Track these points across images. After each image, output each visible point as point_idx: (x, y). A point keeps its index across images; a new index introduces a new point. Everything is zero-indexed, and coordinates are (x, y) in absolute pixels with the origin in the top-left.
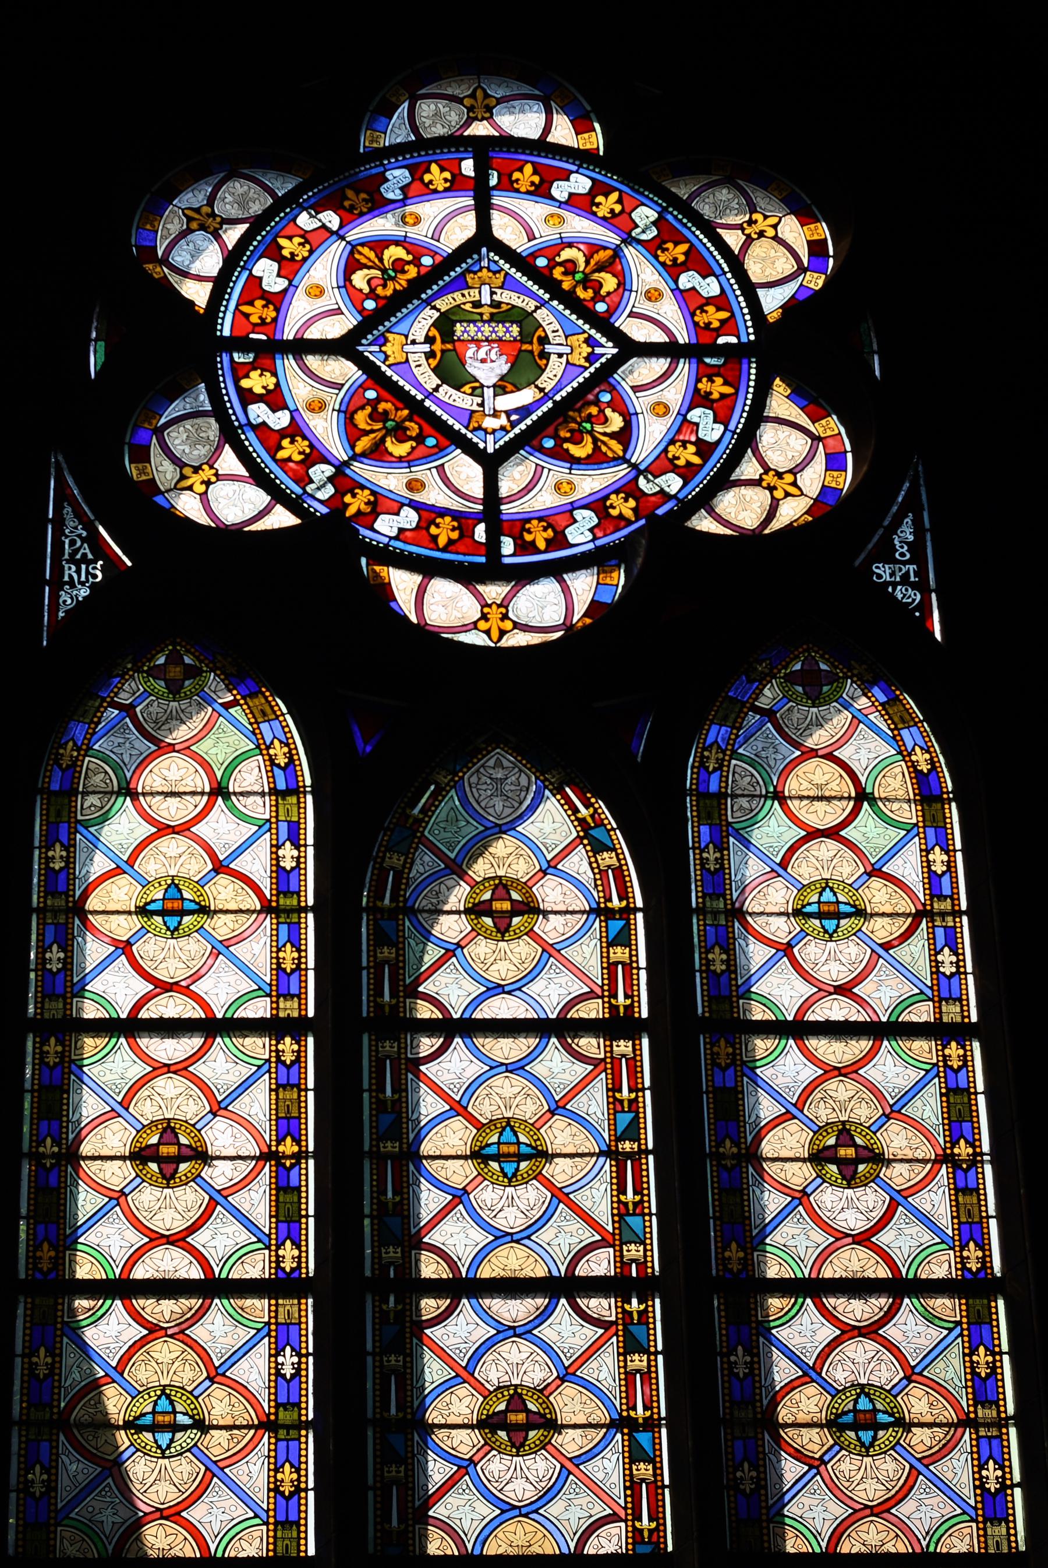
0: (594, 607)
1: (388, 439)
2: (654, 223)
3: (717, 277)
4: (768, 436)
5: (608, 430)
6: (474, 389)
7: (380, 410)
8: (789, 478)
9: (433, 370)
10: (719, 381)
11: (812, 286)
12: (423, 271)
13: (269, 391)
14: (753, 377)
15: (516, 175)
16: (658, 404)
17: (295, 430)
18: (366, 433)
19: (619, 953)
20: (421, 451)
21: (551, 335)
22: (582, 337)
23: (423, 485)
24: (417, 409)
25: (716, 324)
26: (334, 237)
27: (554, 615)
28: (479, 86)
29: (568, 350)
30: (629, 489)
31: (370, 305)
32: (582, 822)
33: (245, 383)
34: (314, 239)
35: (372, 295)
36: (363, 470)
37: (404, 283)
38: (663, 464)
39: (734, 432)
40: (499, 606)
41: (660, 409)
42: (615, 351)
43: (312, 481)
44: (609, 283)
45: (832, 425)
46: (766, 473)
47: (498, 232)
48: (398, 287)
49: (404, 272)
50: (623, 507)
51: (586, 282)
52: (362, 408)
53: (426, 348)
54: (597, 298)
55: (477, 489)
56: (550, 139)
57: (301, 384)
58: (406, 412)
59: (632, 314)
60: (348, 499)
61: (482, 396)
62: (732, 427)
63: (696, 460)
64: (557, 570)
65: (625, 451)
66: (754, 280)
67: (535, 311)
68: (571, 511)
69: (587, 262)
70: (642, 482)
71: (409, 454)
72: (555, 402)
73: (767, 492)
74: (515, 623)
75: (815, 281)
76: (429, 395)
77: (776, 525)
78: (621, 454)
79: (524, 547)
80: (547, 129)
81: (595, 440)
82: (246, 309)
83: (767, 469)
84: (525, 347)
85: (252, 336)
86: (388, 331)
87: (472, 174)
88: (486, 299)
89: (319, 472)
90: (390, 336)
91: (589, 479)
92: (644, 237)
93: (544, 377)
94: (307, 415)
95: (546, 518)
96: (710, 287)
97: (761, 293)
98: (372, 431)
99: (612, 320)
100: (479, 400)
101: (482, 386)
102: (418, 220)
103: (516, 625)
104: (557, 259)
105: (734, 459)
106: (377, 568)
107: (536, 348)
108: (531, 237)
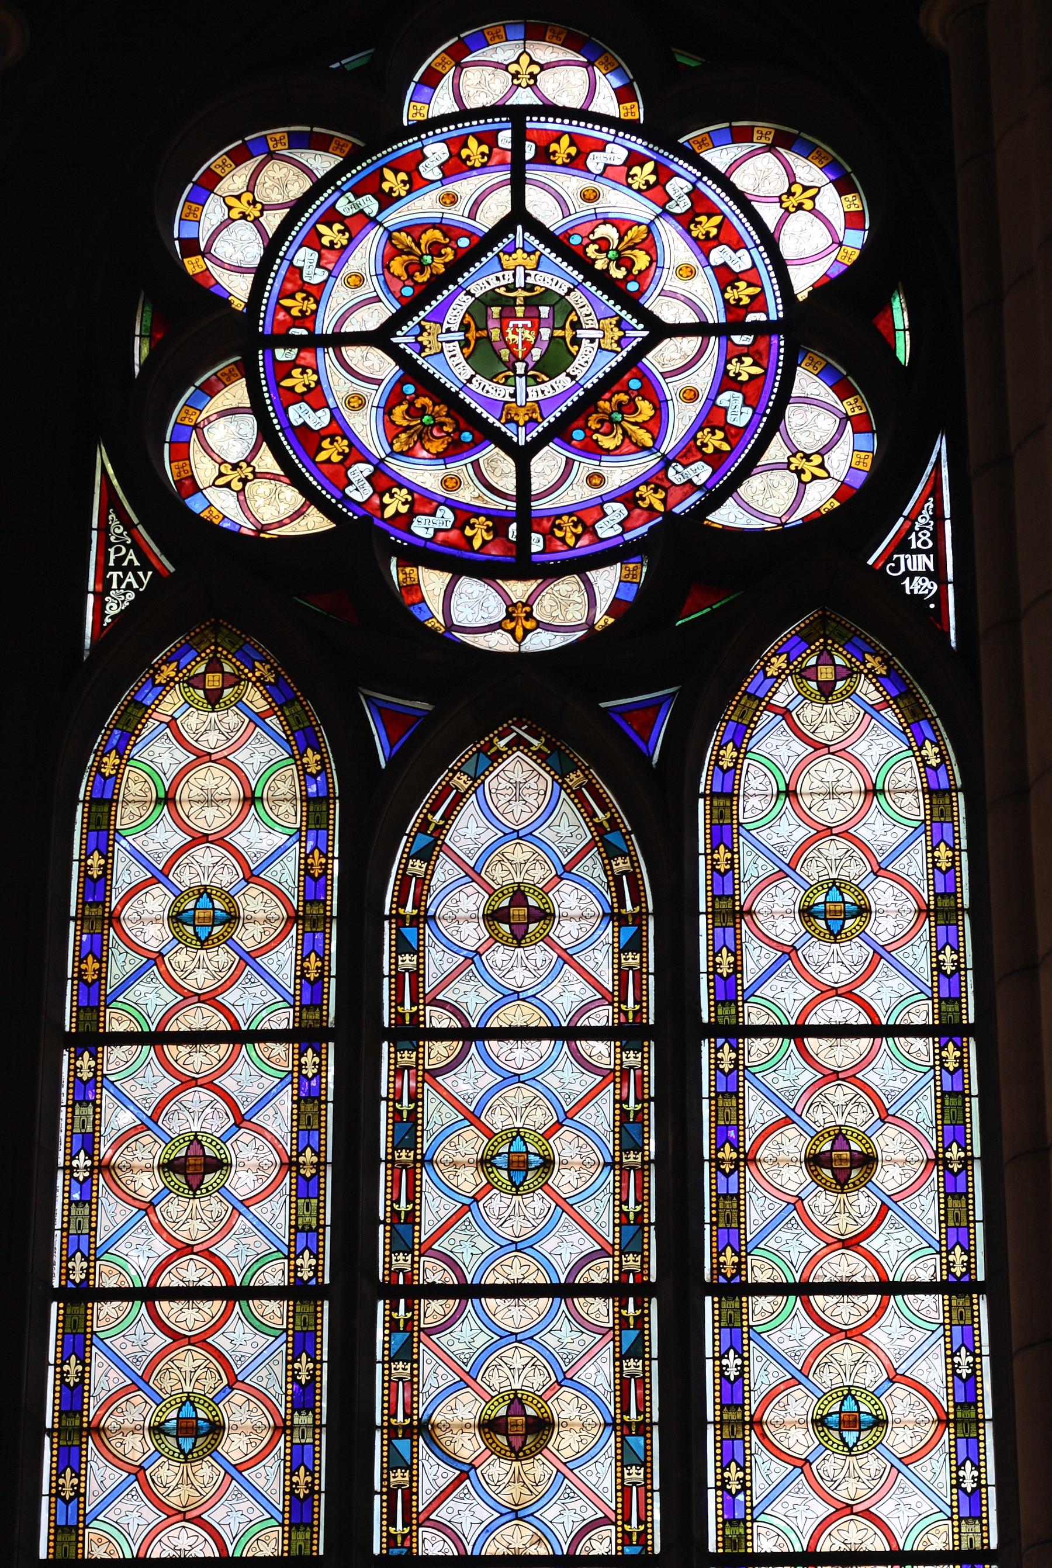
4: (794, 415)
8: (817, 460)
19: (632, 960)
25: (746, 301)
32: (599, 826)
42: (645, 333)
44: (642, 261)
53: (460, 336)
61: (515, 386)
69: (621, 239)
72: (585, 390)
73: (795, 475)
84: (558, 333)
88: (520, 282)
91: (619, 470)
92: (677, 210)
93: (576, 363)
99: (642, 301)
103: (539, 624)
104: (591, 237)
106: (408, 570)
107: (569, 334)
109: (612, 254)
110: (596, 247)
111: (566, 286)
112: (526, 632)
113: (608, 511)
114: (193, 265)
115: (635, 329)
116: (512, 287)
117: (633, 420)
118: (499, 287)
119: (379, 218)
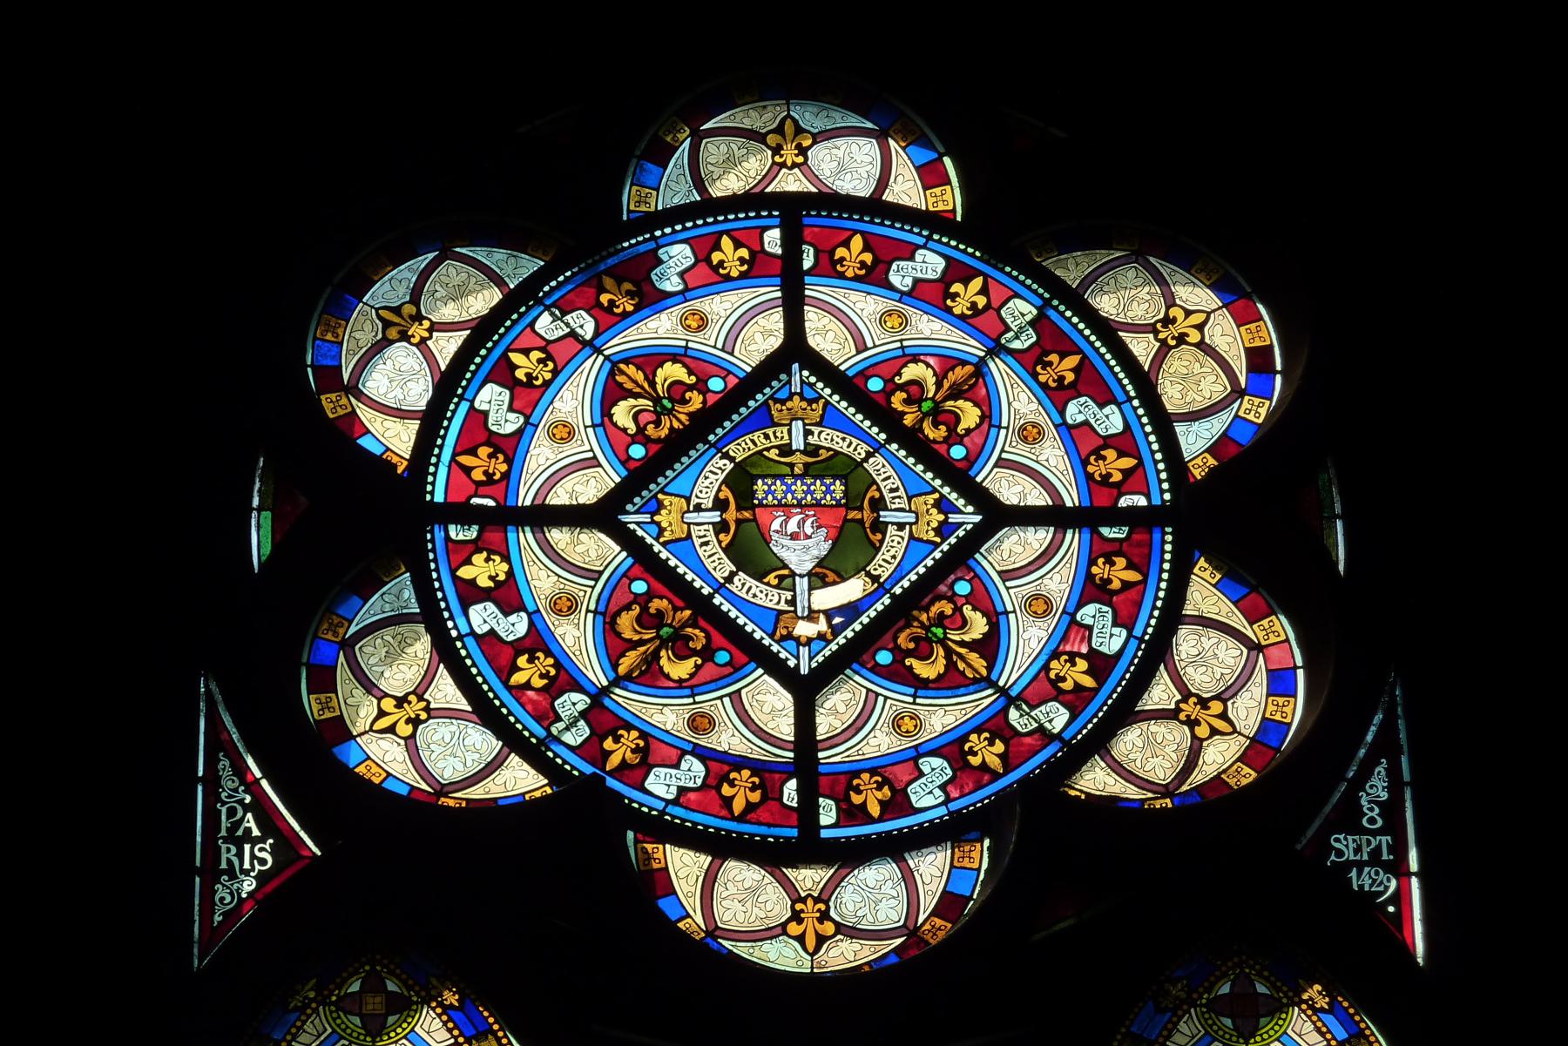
0: (949, 903)
1: (663, 653)
2: (1032, 323)
3: (1119, 405)
4: (1186, 642)
5: (967, 638)
6: (781, 578)
7: (652, 611)
8: (1216, 707)
9: (726, 550)
10: (1121, 562)
11: (1251, 417)
12: (711, 399)
13: (498, 584)
14: (1168, 556)
15: (841, 252)
16: (1037, 597)
17: (537, 642)
18: (634, 645)
20: (709, 671)
21: (888, 496)
22: (931, 499)
23: (712, 723)
24: (703, 609)
25: (1117, 477)
26: (587, 351)
27: (890, 913)
28: (789, 116)
29: (911, 518)
30: (996, 727)
31: (637, 451)
33: (465, 572)
34: (559, 352)
35: (640, 436)
36: (628, 701)
37: (683, 418)
38: (1045, 687)
39: (1141, 640)
40: (817, 900)
41: (1038, 605)
42: (977, 518)
43: (558, 719)
44: (970, 415)
45: (1277, 627)
46: (1185, 700)
47: (813, 341)
48: (676, 424)
49: (685, 402)
50: (988, 753)
51: (938, 415)
52: (628, 608)
53: (715, 517)
54: (953, 438)
55: (785, 728)
56: (888, 197)
57: (543, 574)
58: (688, 613)
59: (1001, 464)
60: (608, 744)
61: (794, 590)
62: (1138, 632)
63: (1088, 682)
64: (896, 848)
65: (990, 668)
66: (1170, 408)
67: (866, 460)
68: (915, 760)
69: (939, 385)
70: (1013, 714)
71: (692, 675)
72: (893, 596)
73: (1186, 728)
74: (837, 924)
75: (1257, 411)
76: (719, 588)
77: (1198, 777)
78: (984, 672)
79: (851, 814)
80: (883, 182)
81: (949, 653)
82: (466, 460)
83: (1186, 695)
84: (852, 515)
85: (475, 501)
86: (662, 491)
87: (779, 251)
88: (798, 443)
89: (568, 705)
90: (667, 500)
92: (1016, 345)
94: (550, 619)
95: (879, 770)
96: (1111, 421)
97: (1180, 428)
98: (641, 643)
100: (789, 595)
101: (793, 574)
102: (704, 322)
103: (840, 928)
105: (1141, 681)
106: (649, 847)
107: (867, 515)
108: (861, 347)
109: (926, 406)
110: (904, 395)
111: (863, 449)
112: (821, 940)
113: (926, 769)
114: (331, 405)
115: (961, 512)
116: (787, 449)
117: (957, 638)
118: (768, 449)
119: (598, 343)
